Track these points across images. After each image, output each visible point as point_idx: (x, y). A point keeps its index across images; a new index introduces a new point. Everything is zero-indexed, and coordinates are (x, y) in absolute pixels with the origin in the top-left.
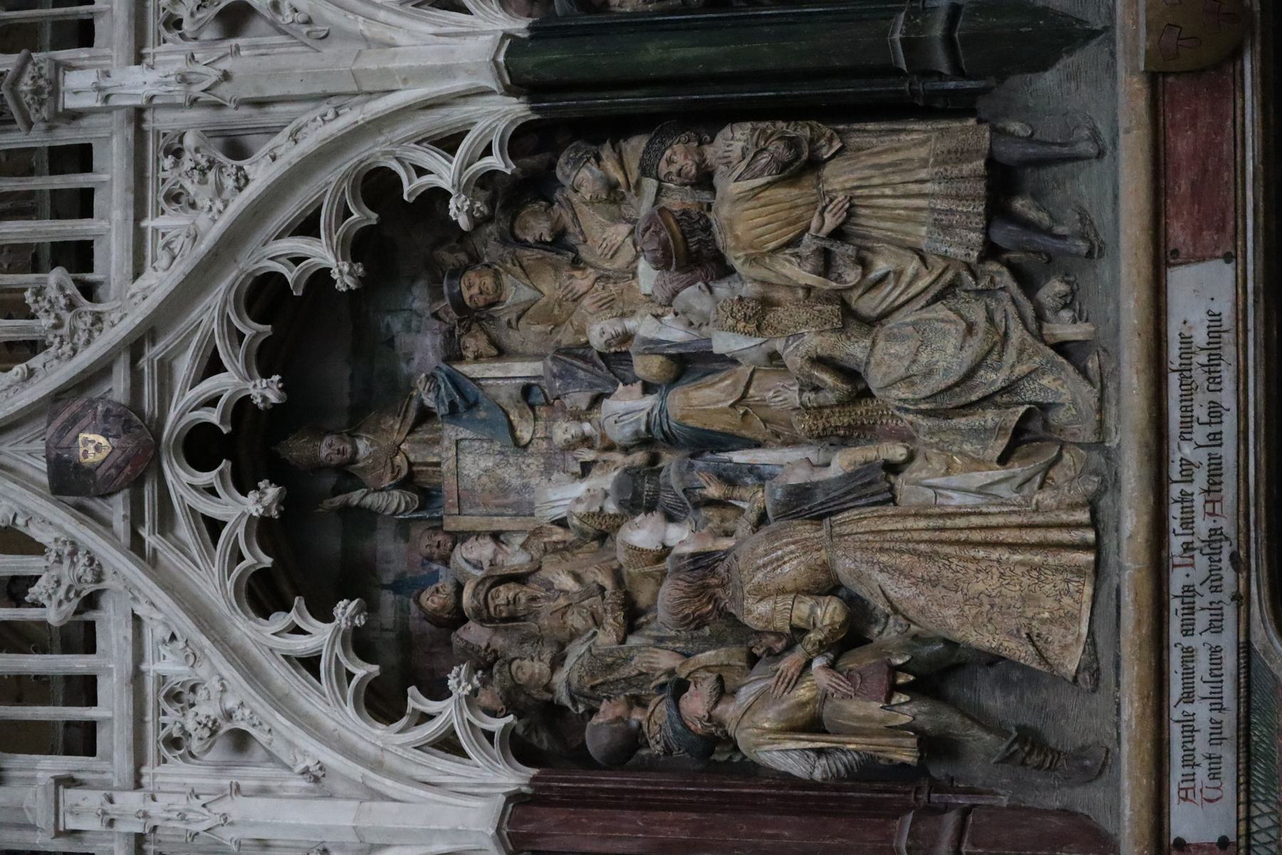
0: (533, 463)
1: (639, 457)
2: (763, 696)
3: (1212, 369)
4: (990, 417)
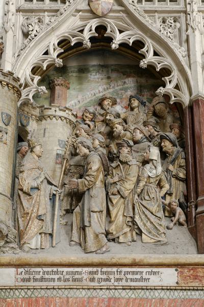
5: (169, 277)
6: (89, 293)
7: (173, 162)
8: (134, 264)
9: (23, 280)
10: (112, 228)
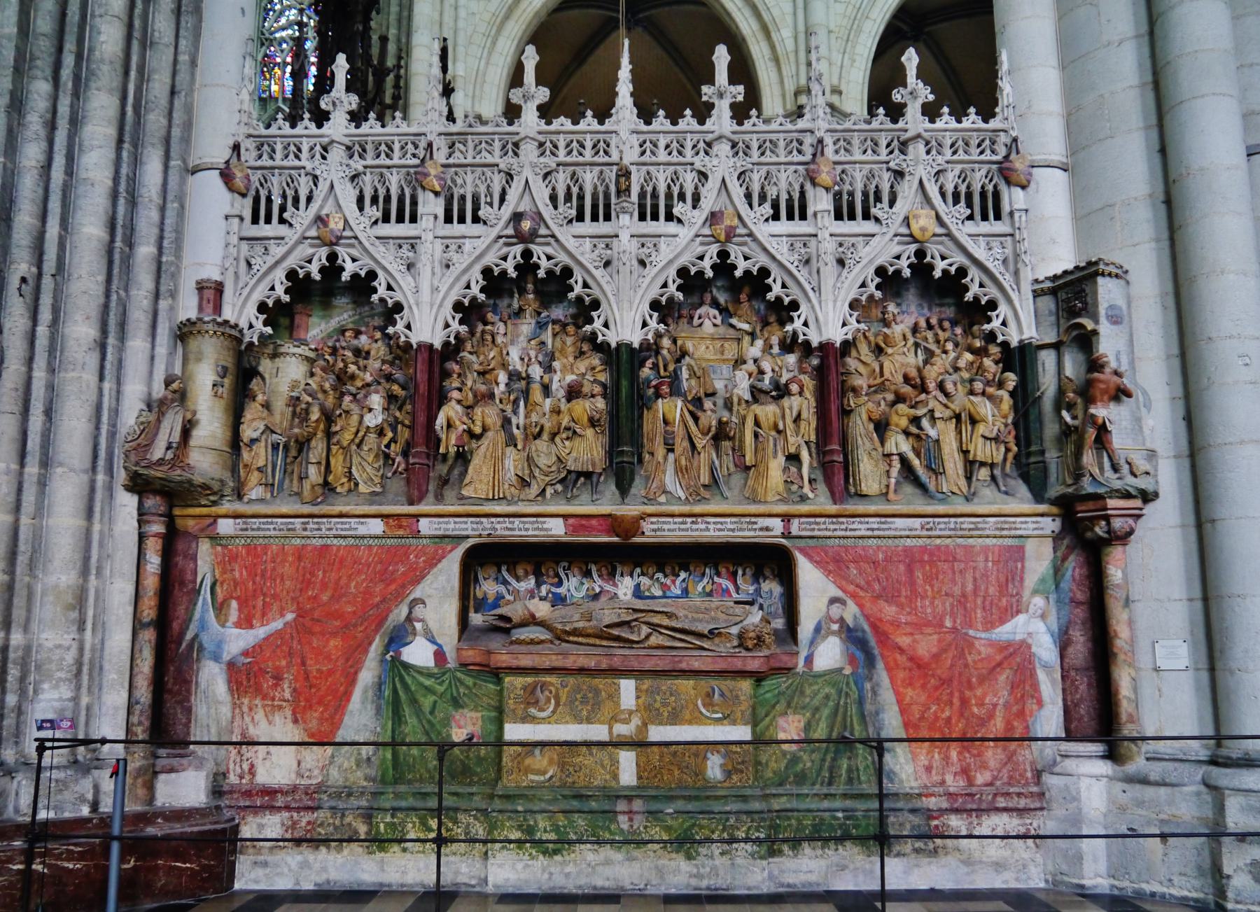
0: (525, 345)
1: (524, 375)
2: (457, 412)
3: (538, 529)
4: (527, 472)
5: (376, 526)
6: (303, 541)
7: (400, 409)
8: (341, 516)
9: (242, 530)
10: (330, 479)
